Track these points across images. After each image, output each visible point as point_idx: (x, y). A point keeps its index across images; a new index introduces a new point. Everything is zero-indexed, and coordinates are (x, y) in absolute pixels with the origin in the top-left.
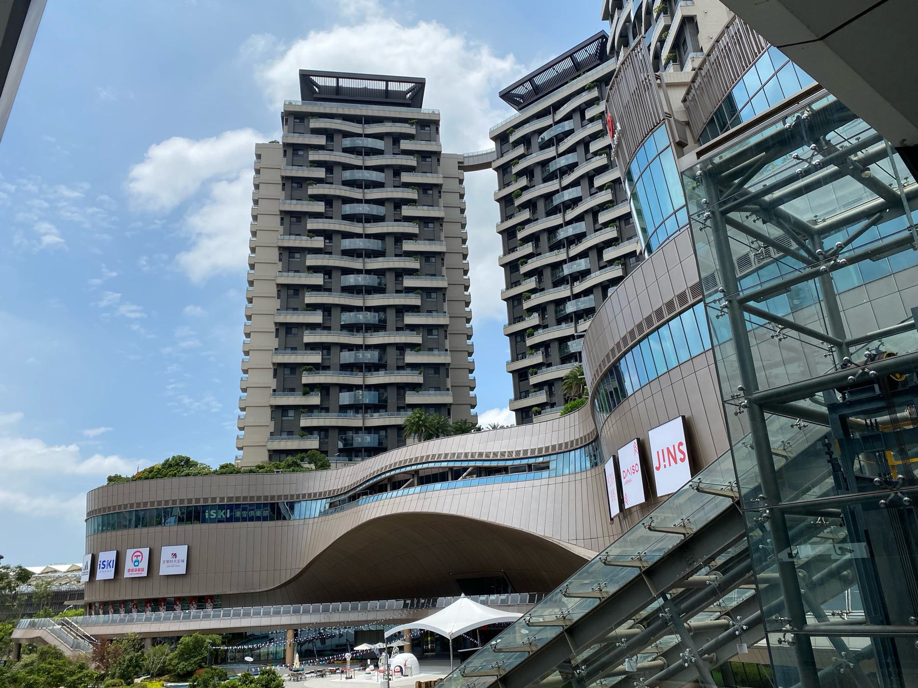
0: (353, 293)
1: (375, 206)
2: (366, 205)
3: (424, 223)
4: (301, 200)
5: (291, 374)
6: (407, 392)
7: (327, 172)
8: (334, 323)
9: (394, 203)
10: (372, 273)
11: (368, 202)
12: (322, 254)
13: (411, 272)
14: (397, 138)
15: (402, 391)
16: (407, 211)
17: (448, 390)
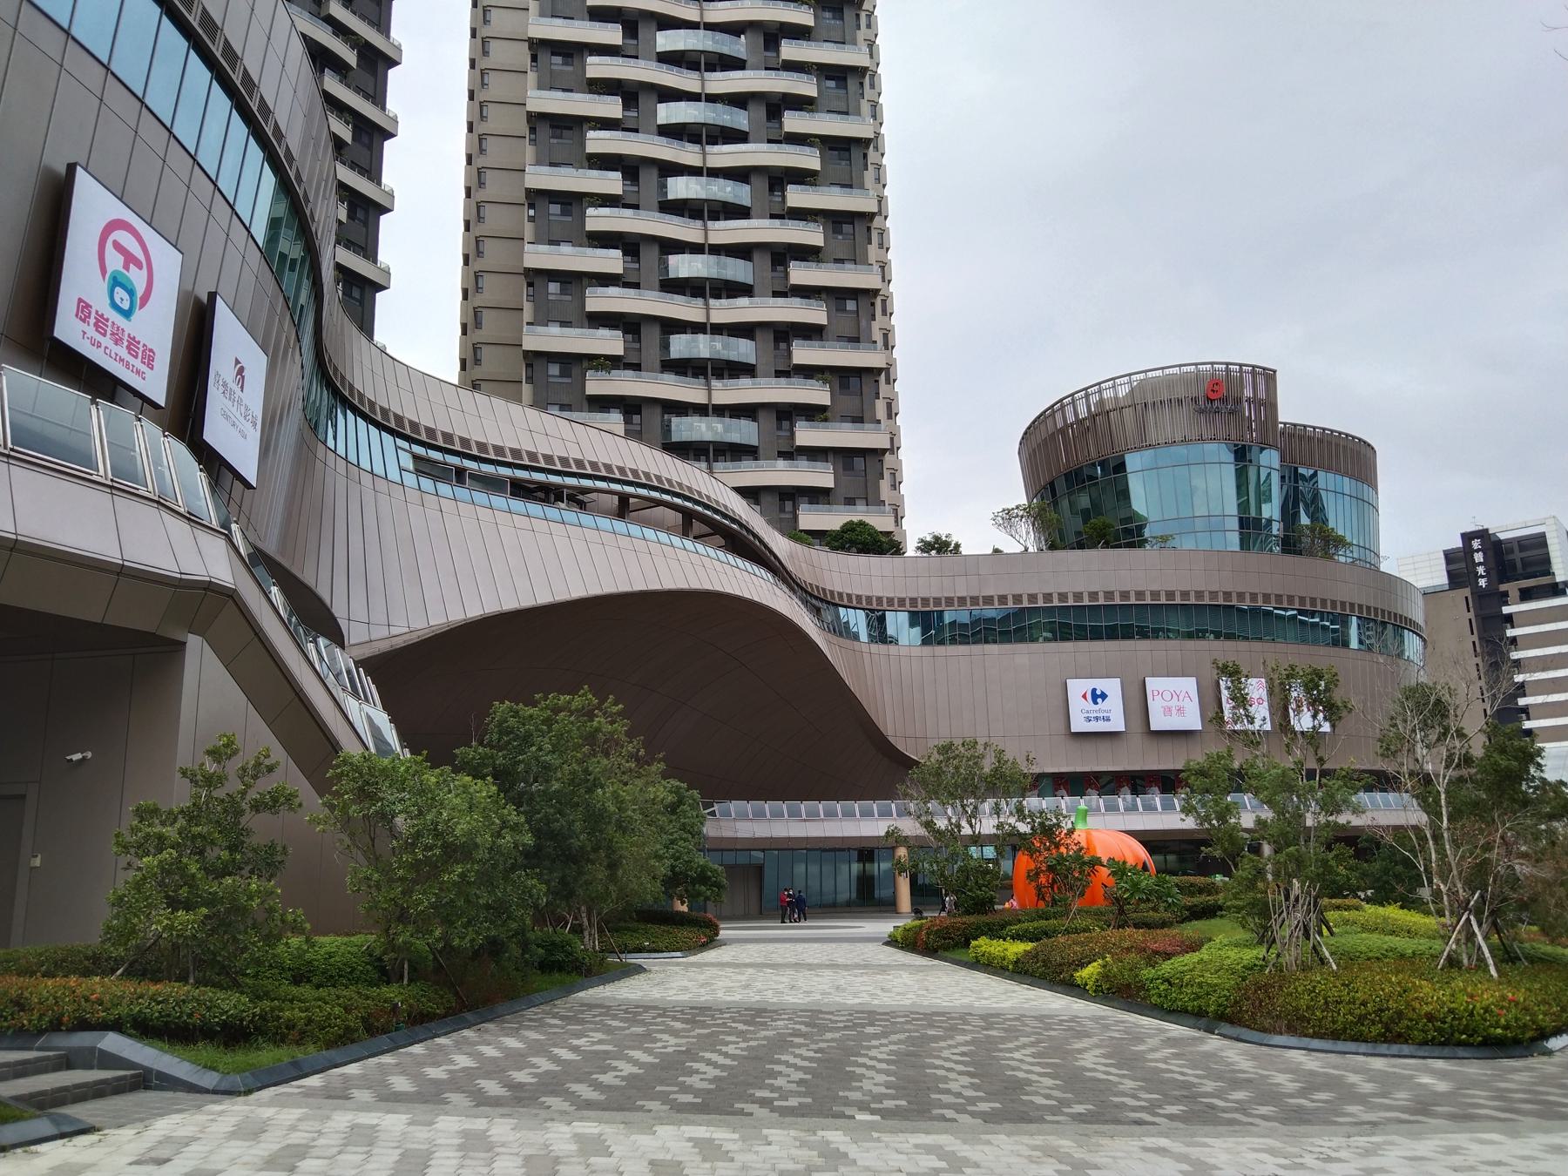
0: (685, 374)
1: (730, 260)
2: (713, 259)
3: (833, 222)
4: (572, 18)
5: (561, 376)
6: (802, 507)
7: (626, 107)
8: (651, 353)
9: (775, 331)
10: (727, 414)
11: (721, 411)
12: (618, 207)
13: (812, 413)
14: (779, 254)
15: (789, 505)
16: (800, 274)
17: (879, 422)
